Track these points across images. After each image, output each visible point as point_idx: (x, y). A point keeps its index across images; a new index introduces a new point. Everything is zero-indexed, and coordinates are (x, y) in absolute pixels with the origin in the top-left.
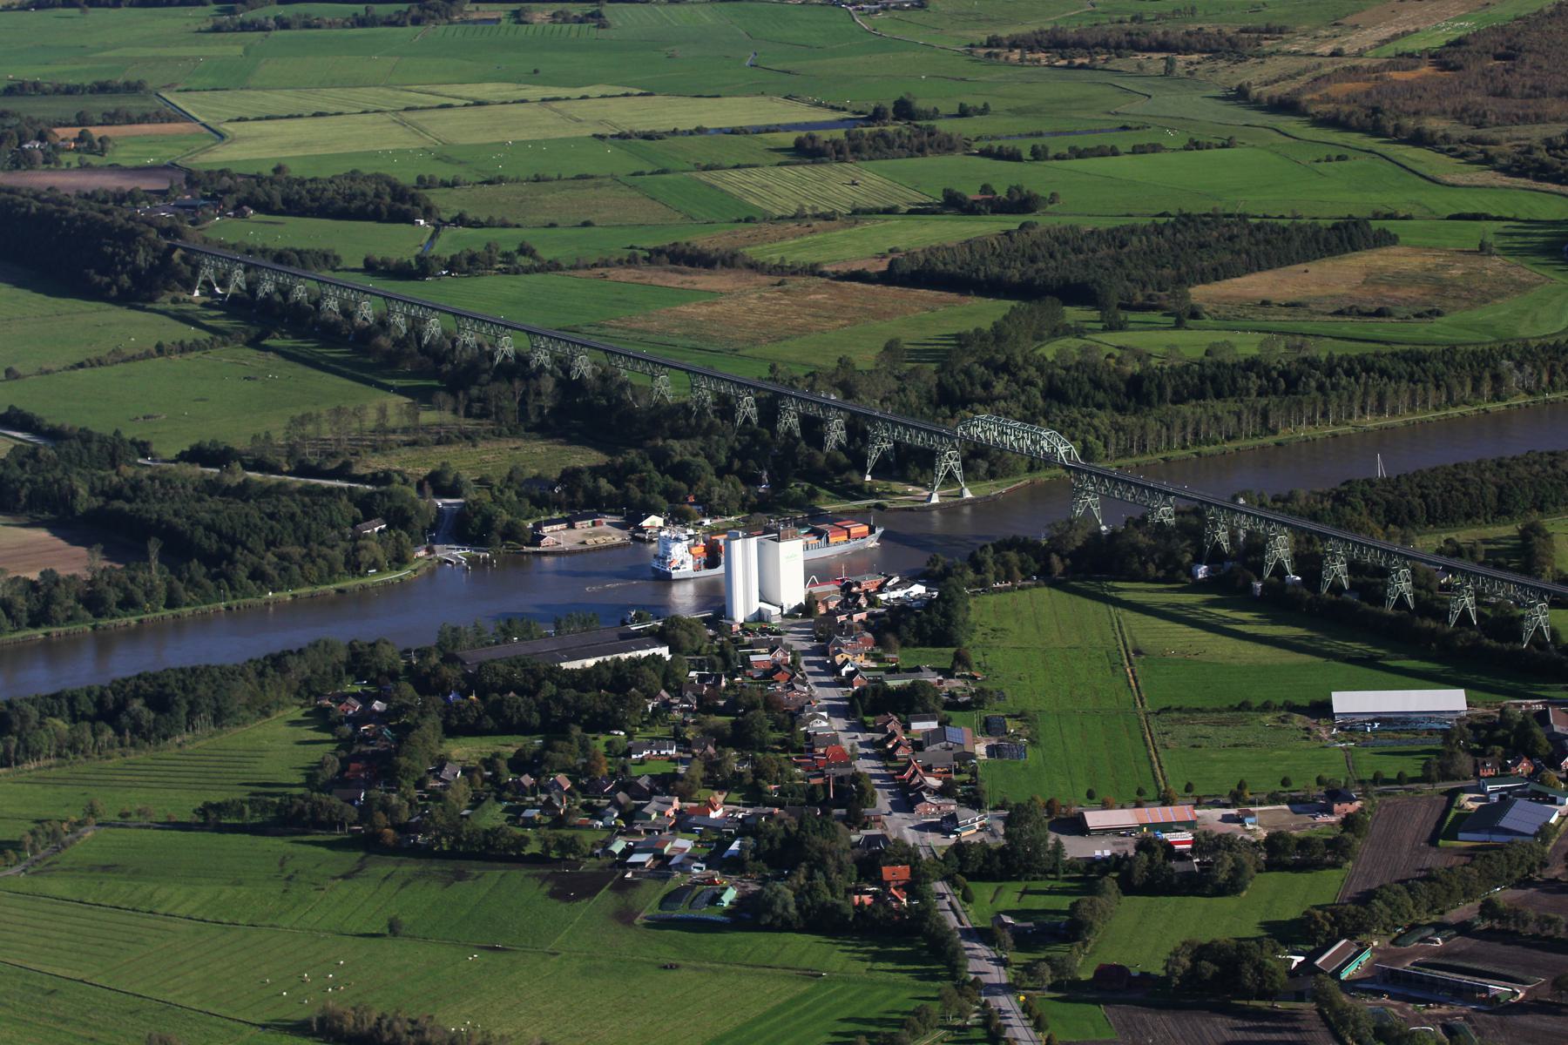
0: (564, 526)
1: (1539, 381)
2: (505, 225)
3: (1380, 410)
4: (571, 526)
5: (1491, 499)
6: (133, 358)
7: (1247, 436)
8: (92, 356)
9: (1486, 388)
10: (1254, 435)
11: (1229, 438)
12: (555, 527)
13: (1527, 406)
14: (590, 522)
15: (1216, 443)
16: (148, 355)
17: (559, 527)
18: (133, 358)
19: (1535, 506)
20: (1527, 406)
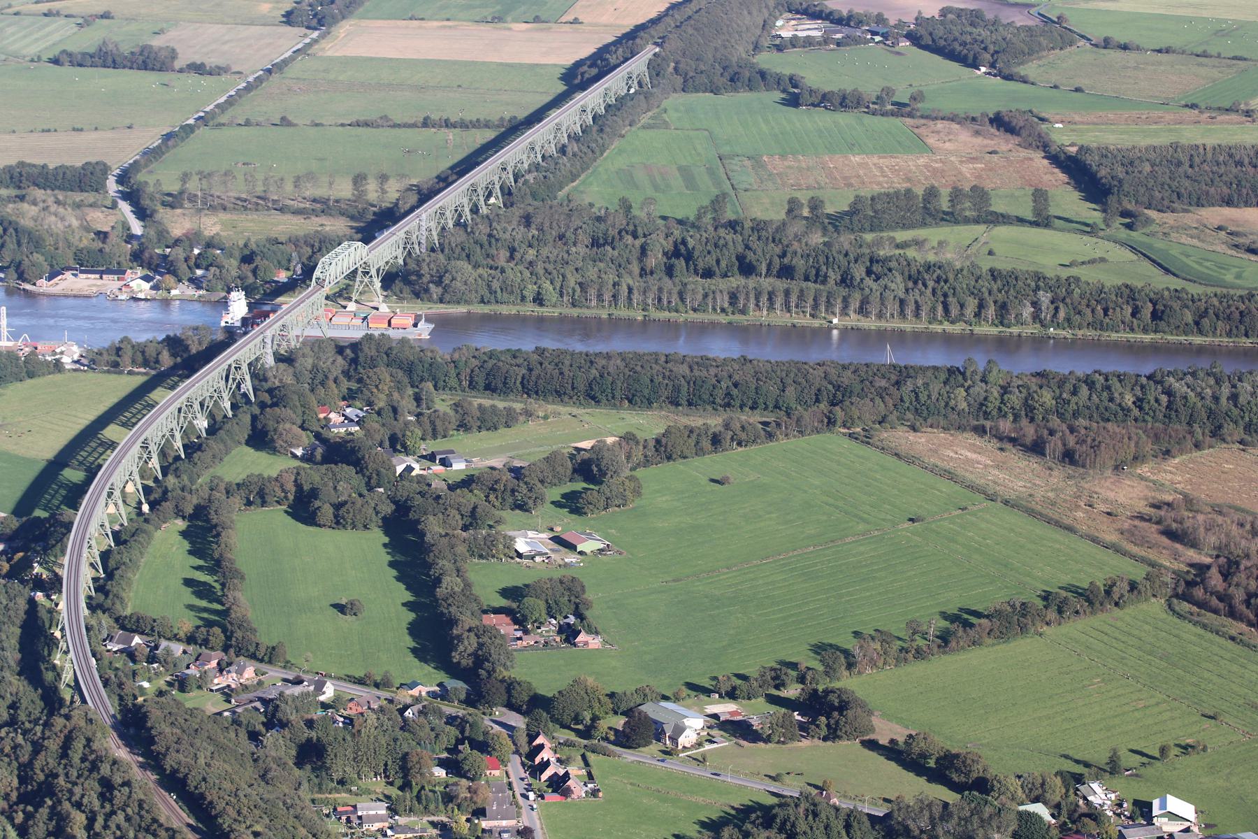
0: (98, 276)
1: (1055, 315)
2: (1025, 82)
3: (862, 310)
4: (101, 278)
5: (582, 387)
6: (399, 126)
7: (714, 309)
8: (362, 118)
9: (991, 311)
10: (723, 310)
11: (695, 310)
12: (89, 276)
13: (1019, 336)
14: (116, 277)
15: (677, 311)
16: (414, 126)
17: (93, 276)
18: (399, 126)
19: (627, 399)
20: (1019, 336)
